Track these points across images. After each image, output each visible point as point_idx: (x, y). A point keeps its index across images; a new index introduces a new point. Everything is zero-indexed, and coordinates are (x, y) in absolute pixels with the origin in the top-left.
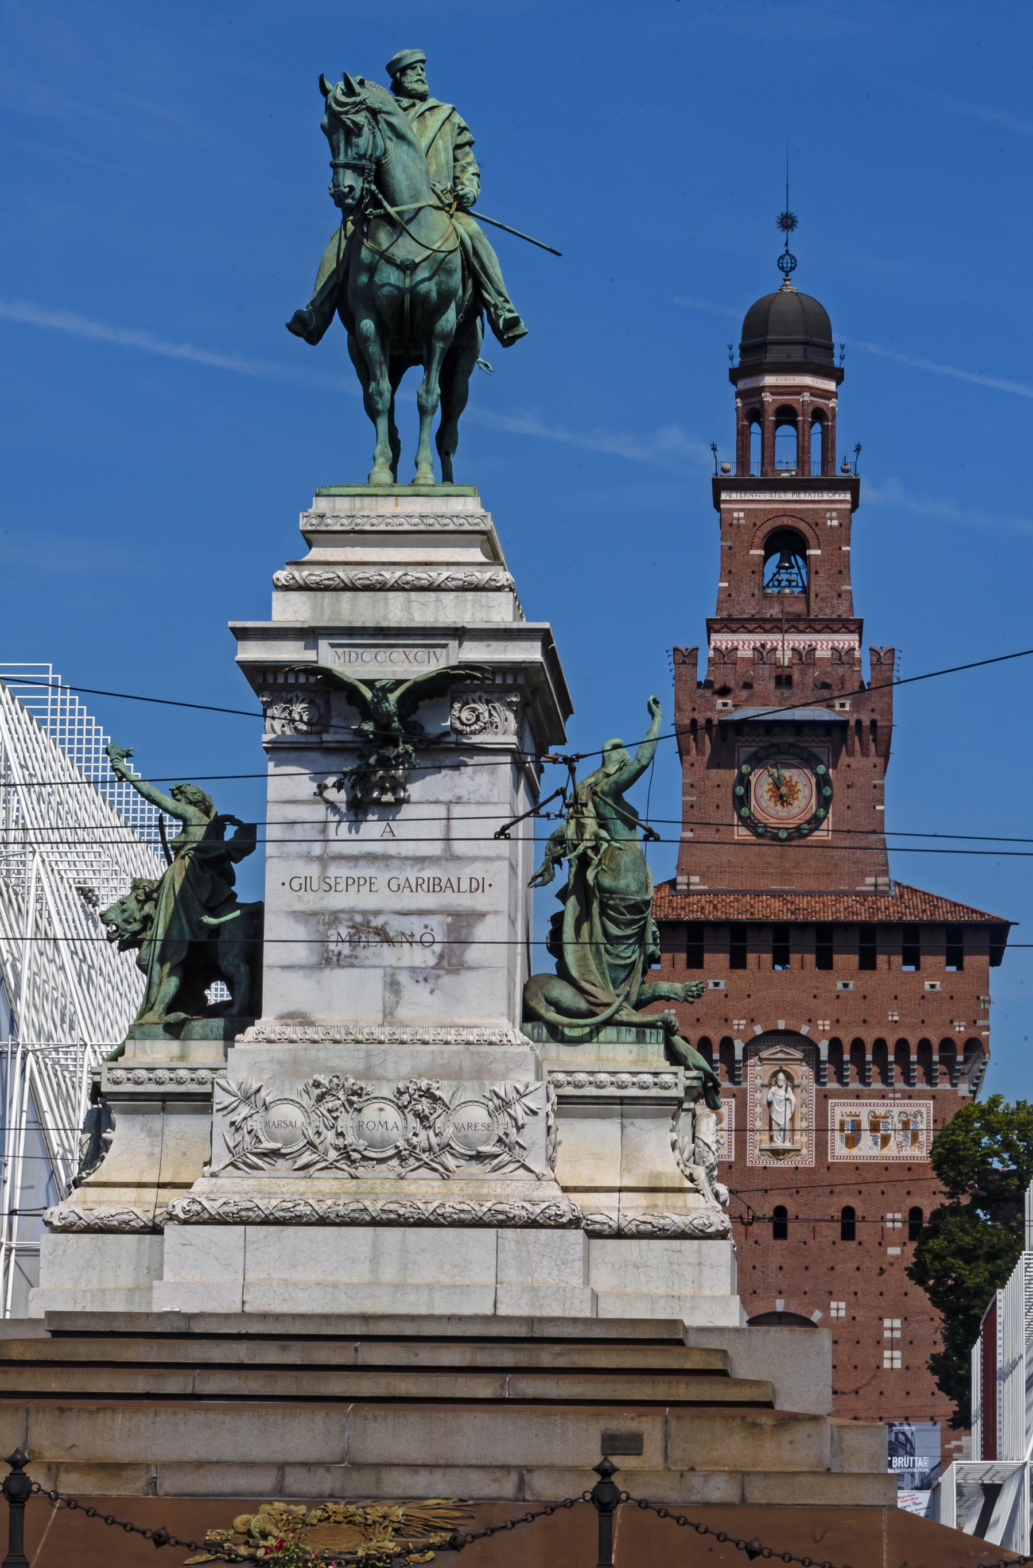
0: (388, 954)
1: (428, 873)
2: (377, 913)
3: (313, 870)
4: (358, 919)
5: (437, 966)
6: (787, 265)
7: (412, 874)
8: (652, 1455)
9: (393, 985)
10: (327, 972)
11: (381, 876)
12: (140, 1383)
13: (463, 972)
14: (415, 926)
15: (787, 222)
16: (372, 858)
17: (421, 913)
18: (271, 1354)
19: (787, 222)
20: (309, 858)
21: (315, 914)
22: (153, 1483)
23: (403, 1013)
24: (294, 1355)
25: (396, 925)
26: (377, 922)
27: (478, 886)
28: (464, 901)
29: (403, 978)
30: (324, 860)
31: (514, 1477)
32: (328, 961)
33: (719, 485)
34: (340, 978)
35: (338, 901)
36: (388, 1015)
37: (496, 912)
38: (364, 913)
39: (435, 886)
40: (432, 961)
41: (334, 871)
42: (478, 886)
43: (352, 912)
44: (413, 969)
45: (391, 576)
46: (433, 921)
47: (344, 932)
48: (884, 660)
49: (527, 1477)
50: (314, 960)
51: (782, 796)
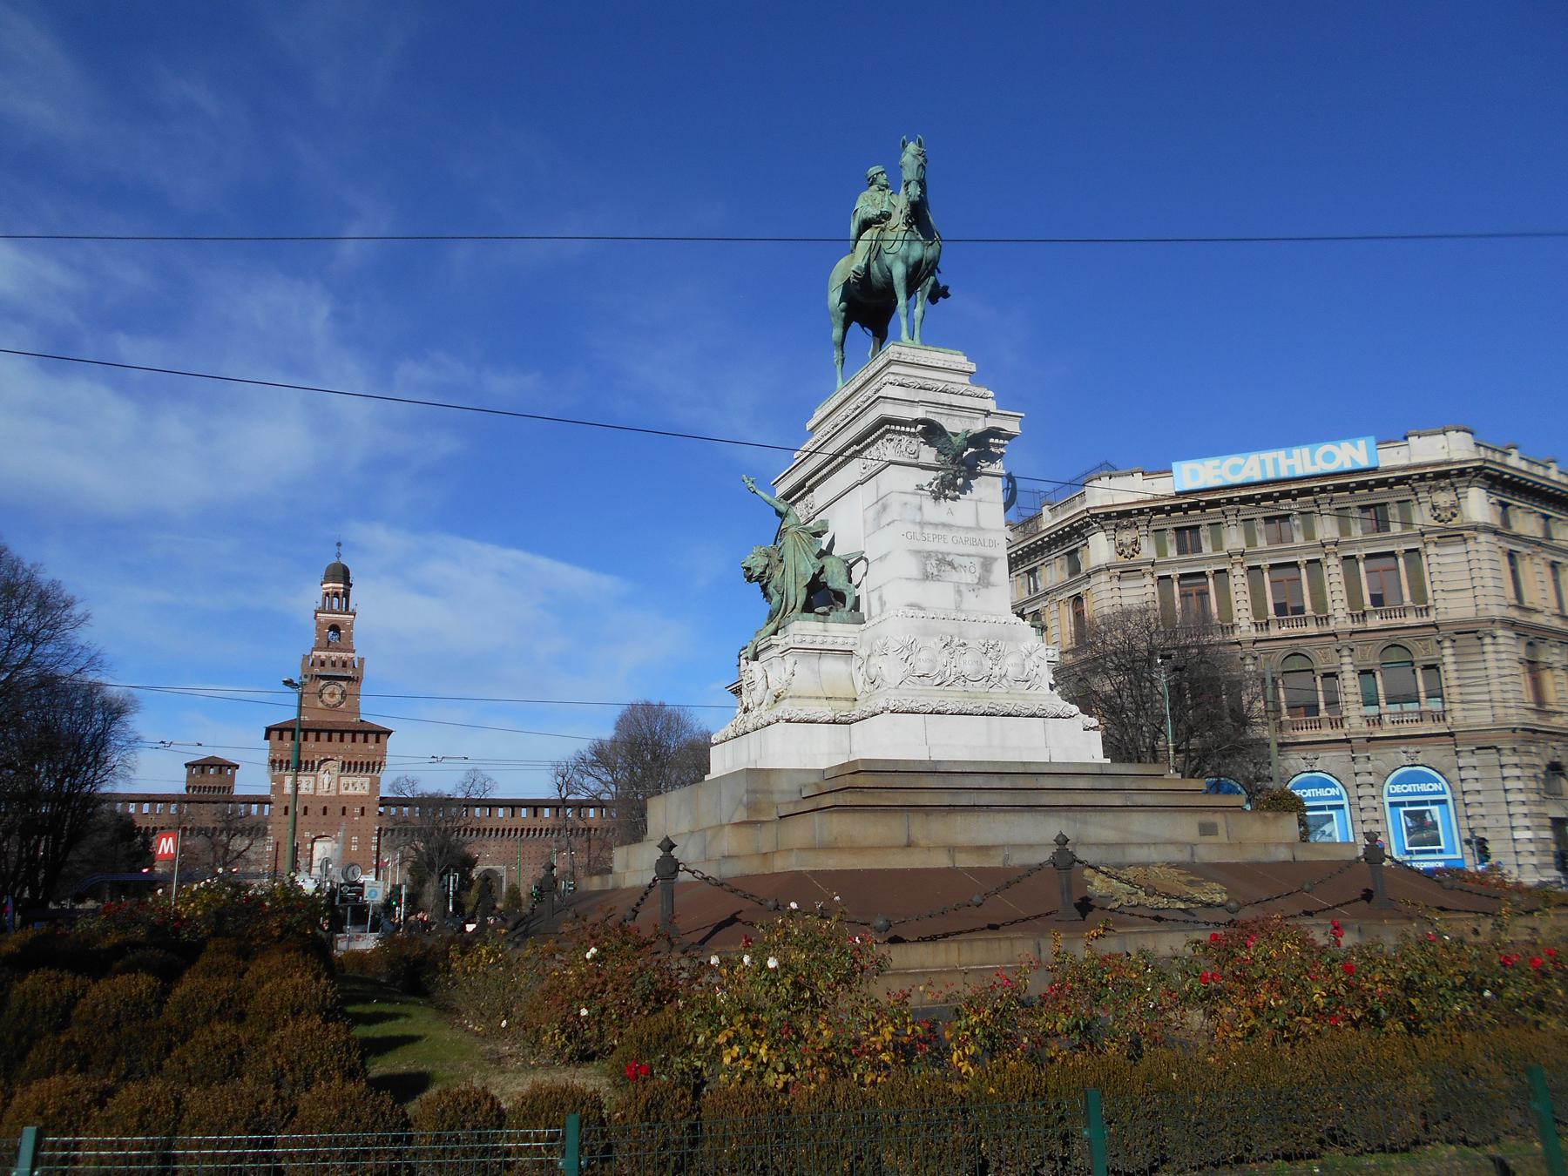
0: (955, 576)
1: (971, 535)
2: (949, 554)
3: (917, 529)
4: (940, 556)
5: (977, 584)
6: (339, 555)
7: (962, 535)
8: (1222, 837)
9: (959, 592)
10: (930, 584)
11: (949, 535)
12: (946, 799)
13: (992, 589)
14: (965, 561)
15: (339, 544)
16: (944, 525)
17: (968, 555)
18: (995, 782)
19: (339, 544)
20: (914, 522)
21: (919, 552)
22: (1007, 858)
23: (964, 606)
24: (1006, 783)
25: (957, 561)
26: (949, 558)
27: (994, 544)
28: (989, 552)
29: (963, 588)
30: (922, 524)
31: (1189, 848)
32: (927, 577)
33: (317, 612)
34: (931, 586)
35: (929, 546)
36: (958, 608)
37: (1003, 558)
38: (942, 553)
39: (974, 543)
40: (976, 581)
41: (929, 531)
42: (994, 544)
43: (937, 552)
44: (968, 584)
45: (941, 386)
46: (973, 559)
47: (934, 563)
48: (362, 661)
49: (1195, 848)
50: (920, 577)
51: (332, 695)
